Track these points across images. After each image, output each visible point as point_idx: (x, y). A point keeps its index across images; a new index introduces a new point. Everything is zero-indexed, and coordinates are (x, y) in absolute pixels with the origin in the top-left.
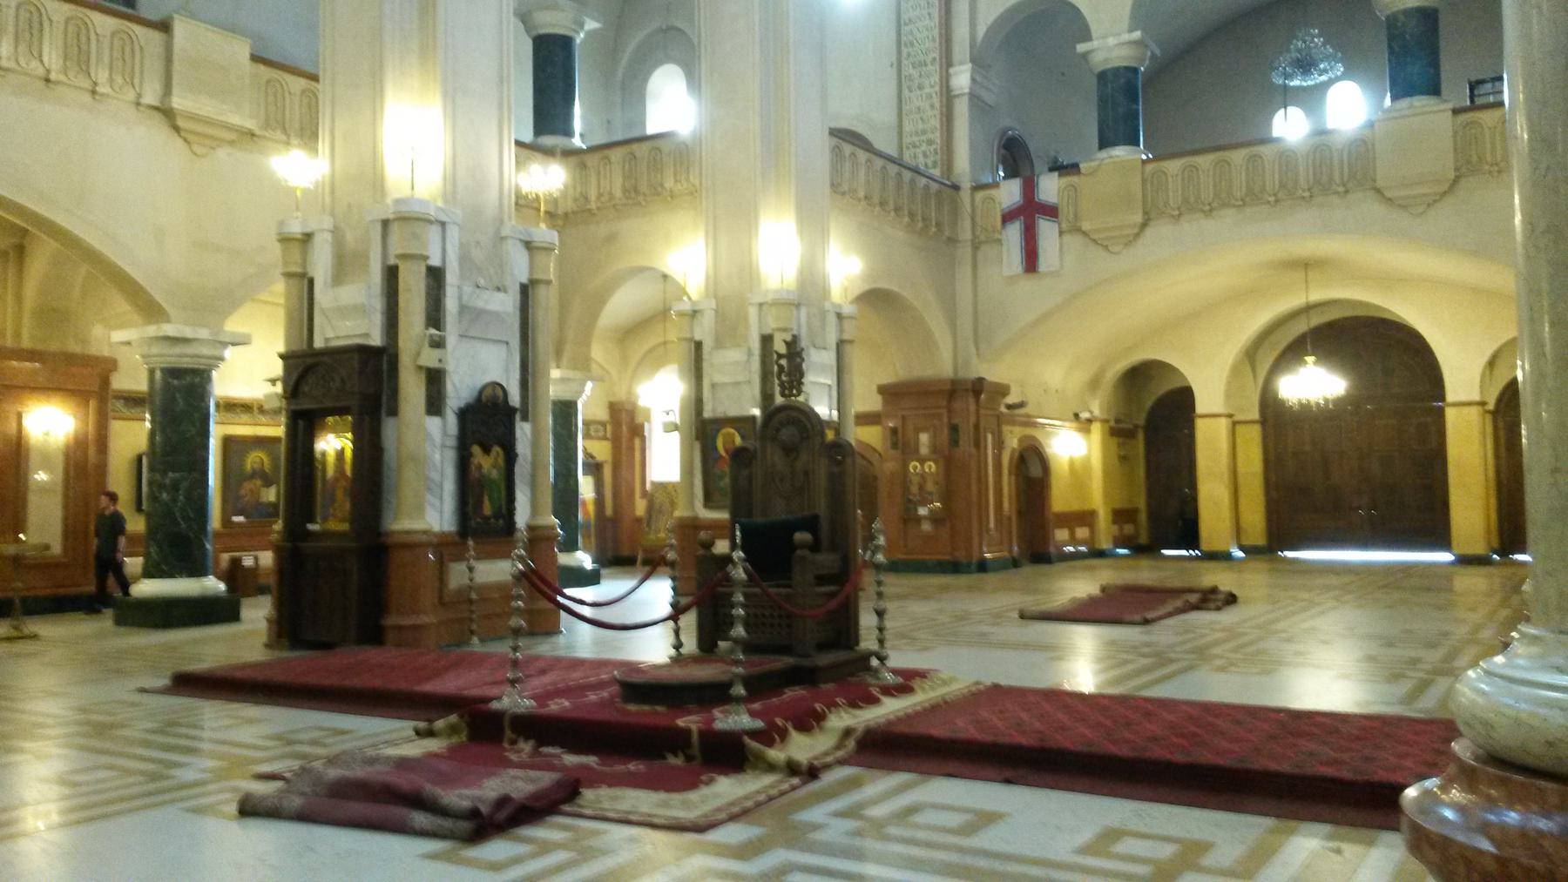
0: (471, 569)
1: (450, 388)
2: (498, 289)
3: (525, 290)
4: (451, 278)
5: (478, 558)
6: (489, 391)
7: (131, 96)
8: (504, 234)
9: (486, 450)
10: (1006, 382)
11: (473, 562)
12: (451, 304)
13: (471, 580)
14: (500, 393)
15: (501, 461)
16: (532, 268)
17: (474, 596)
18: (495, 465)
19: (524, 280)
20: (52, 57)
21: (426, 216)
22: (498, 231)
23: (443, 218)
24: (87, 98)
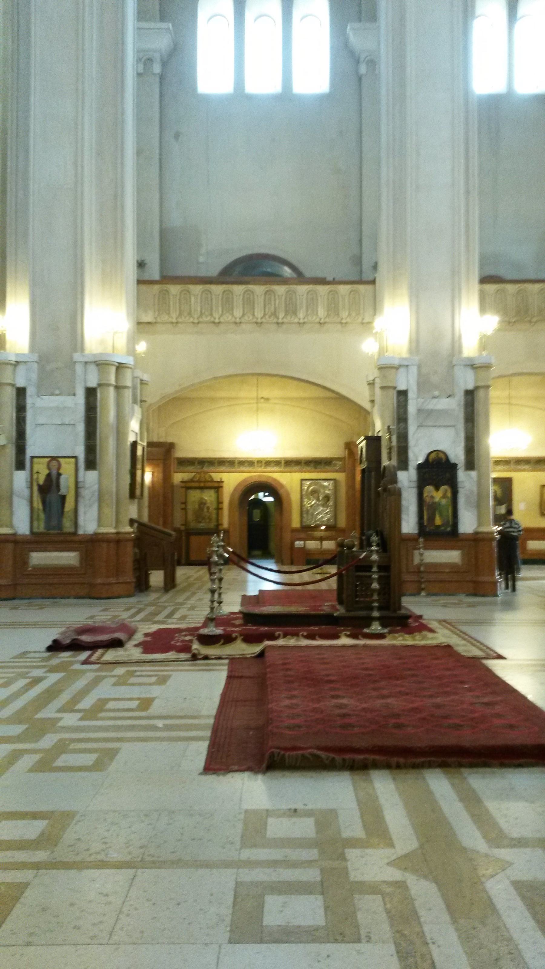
0: (421, 555)
1: (411, 455)
2: (449, 396)
3: (470, 394)
4: (411, 395)
5: (425, 548)
6: (433, 456)
7: (360, 320)
8: (454, 363)
9: (437, 489)
10: (98, 467)
11: (422, 551)
12: (412, 409)
13: (422, 560)
14: (441, 455)
15: (449, 494)
16: (476, 380)
17: (422, 569)
18: (444, 496)
19: (470, 387)
20: (321, 312)
21: (391, 365)
22: (451, 362)
23: (406, 363)
24: (339, 326)
